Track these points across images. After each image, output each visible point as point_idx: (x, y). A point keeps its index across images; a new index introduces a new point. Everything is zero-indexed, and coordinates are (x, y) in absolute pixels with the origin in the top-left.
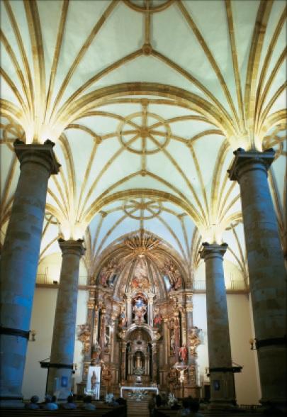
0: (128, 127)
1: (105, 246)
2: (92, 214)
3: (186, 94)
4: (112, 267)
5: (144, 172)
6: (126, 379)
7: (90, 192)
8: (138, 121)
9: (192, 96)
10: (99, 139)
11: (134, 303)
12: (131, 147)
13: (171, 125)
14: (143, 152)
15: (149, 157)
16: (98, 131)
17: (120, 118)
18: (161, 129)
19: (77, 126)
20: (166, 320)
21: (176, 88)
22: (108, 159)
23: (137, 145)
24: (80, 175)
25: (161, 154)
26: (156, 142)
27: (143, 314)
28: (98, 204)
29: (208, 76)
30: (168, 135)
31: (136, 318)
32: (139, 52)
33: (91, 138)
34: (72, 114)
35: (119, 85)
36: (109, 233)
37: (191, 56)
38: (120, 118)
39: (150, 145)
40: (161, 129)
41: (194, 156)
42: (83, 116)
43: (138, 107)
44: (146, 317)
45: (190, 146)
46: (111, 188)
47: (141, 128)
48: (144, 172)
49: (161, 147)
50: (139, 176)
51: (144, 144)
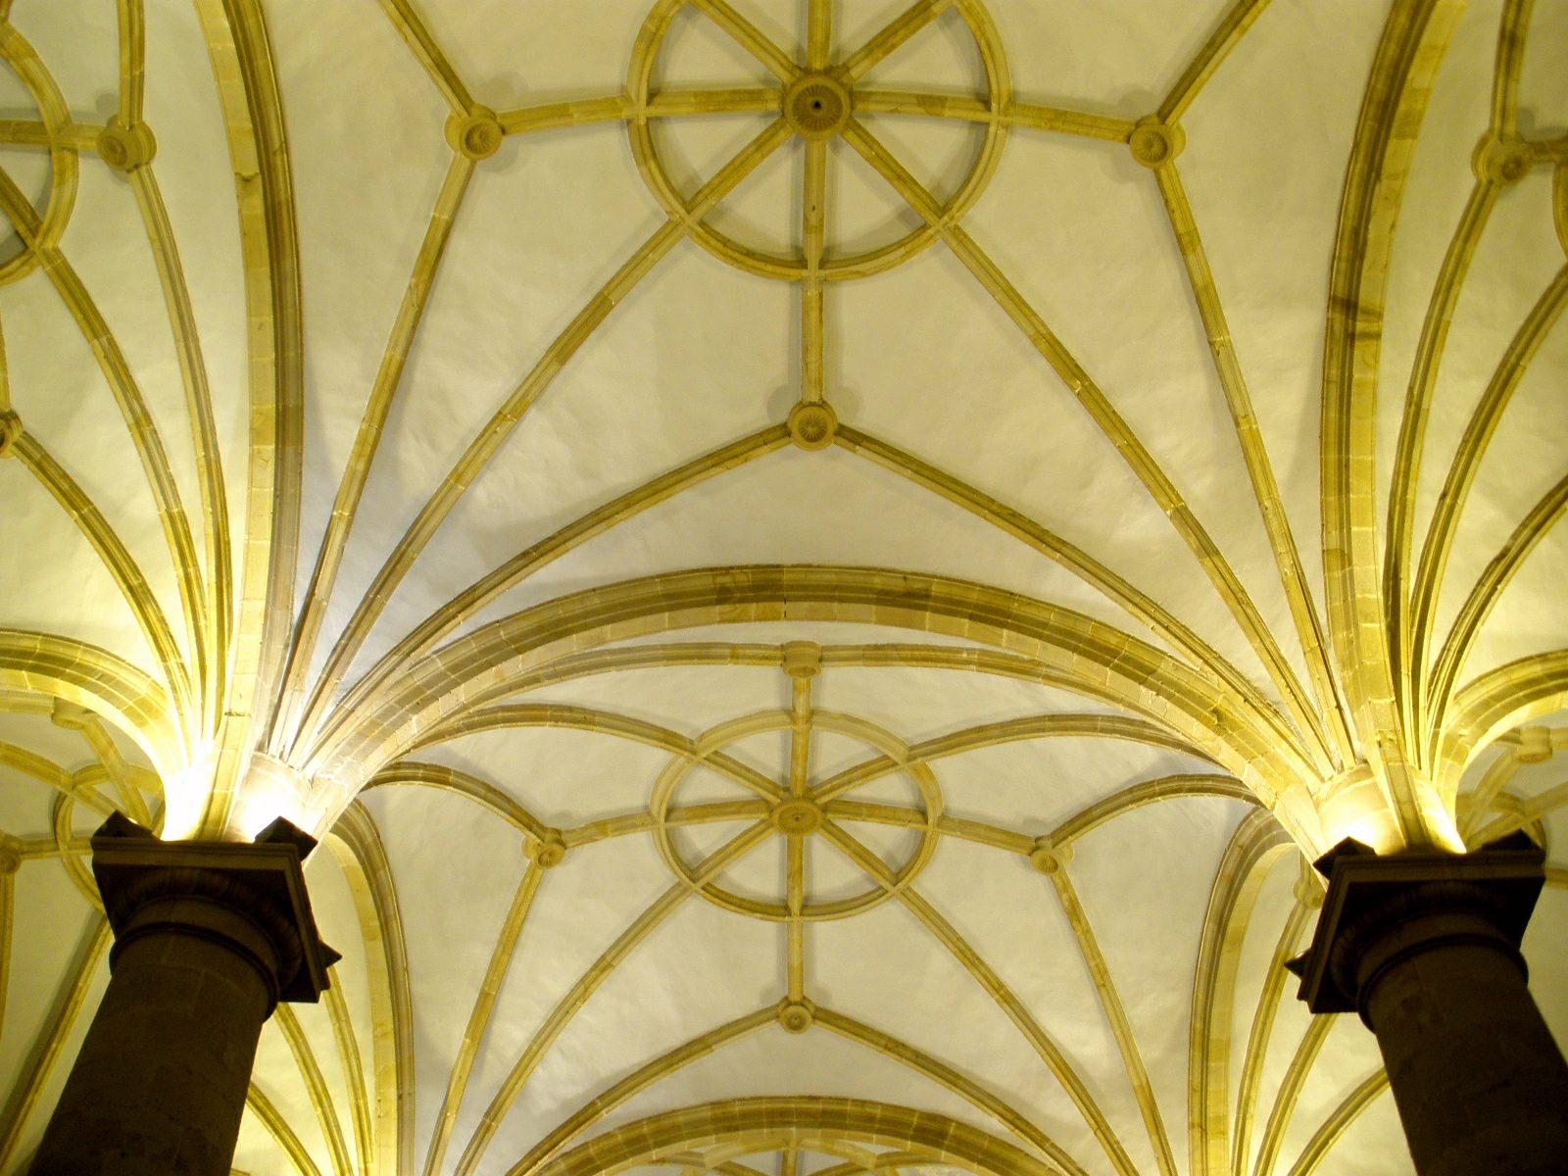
0: (708, 785)
3: (1015, 607)
5: (797, 1011)
7: (493, 1113)
8: (765, 751)
9: (1052, 618)
10: (551, 842)
12: (721, 886)
13: (947, 769)
14: (796, 908)
15: (824, 930)
16: (545, 800)
17: (668, 738)
18: (891, 788)
19: (438, 775)
21: (969, 585)
22: (603, 942)
23: (759, 871)
25: (890, 914)
26: (862, 855)
29: (1138, 528)
30: (924, 816)
32: (780, 433)
33: (510, 841)
34: (418, 708)
35: (665, 577)
37: (1029, 438)
38: (668, 738)
39: (832, 871)
40: (891, 788)
41: (1073, 912)
42: (471, 727)
43: (759, 687)
45: (1052, 867)
46: (613, 1093)
47: (784, 788)
48: (797, 1011)
49: (892, 878)
50: (773, 1033)
51: (795, 868)
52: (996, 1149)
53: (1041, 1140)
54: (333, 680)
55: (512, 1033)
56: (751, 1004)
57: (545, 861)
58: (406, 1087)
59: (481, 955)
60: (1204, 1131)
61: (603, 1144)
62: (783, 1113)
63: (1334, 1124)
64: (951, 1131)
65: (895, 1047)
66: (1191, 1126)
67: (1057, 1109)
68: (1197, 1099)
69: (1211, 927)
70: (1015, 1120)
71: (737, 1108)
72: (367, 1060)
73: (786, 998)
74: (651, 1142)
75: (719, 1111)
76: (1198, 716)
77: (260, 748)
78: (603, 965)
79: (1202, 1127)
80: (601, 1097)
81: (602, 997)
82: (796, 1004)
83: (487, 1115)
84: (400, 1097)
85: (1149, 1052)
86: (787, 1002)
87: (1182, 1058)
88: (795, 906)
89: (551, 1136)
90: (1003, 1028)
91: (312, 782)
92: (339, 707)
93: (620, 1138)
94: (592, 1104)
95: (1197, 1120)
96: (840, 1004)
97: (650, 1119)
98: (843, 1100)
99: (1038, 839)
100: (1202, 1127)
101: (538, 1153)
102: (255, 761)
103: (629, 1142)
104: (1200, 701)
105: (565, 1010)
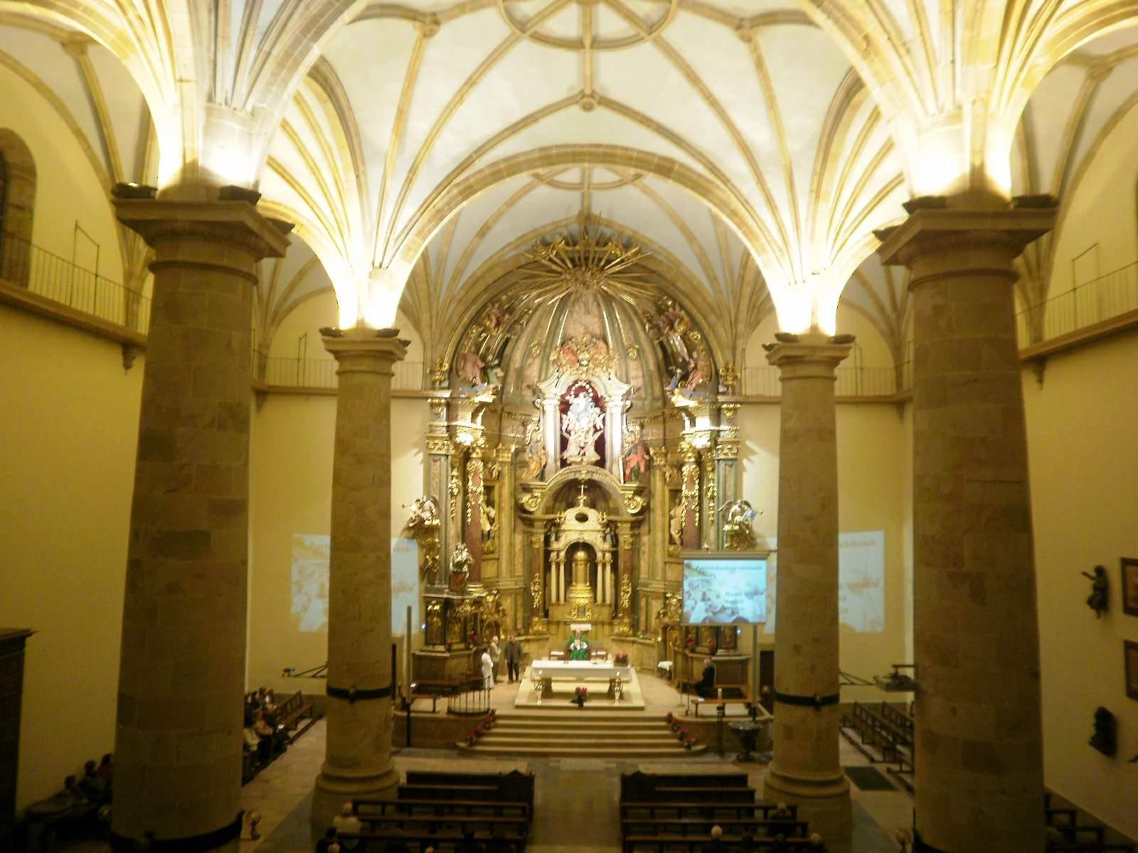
1: (474, 267)
2: (422, 234)
4: (498, 324)
5: (590, 99)
6: (546, 615)
7: (413, 171)
11: (565, 407)
20: (659, 461)
24: (378, 131)
25: (647, 49)
27: (592, 439)
28: (439, 203)
31: (572, 452)
36: (483, 232)
41: (759, 64)
44: (600, 445)
45: (748, 40)
46: (481, 151)
48: (590, 99)
49: (650, 29)
50: (575, 110)
51: (588, 22)
52: (701, 181)
53: (726, 181)
54: (250, 32)
55: (419, 126)
56: (562, 94)
57: (428, 35)
58: (361, 169)
59: (396, 88)
60: (817, 197)
61: (478, 176)
62: (580, 154)
63: (894, 184)
64: (676, 167)
65: (646, 121)
66: (811, 191)
67: (735, 165)
68: (816, 178)
69: (842, 94)
70: (713, 168)
71: (554, 152)
72: (335, 152)
73: (582, 91)
74: (505, 173)
75: (544, 153)
76: (853, 41)
77: (210, 98)
78: (471, 83)
79: (817, 193)
80: (475, 152)
81: (473, 97)
82: (588, 96)
83: (410, 171)
84: (357, 176)
85: (793, 146)
86: (582, 94)
87: (813, 153)
88: (587, 43)
89: (448, 176)
90: (708, 117)
91: (252, 114)
92: (260, 49)
93: (487, 172)
94: (470, 157)
95: (815, 187)
96: (615, 94)
97: (505, 160)
98: (615, 147)
99: (742, 20)
100: (817, 193)
101: (441, 188)
102: (209, 112)
103: (493, 174)
104: (858, 27)
105: (450, 109)
